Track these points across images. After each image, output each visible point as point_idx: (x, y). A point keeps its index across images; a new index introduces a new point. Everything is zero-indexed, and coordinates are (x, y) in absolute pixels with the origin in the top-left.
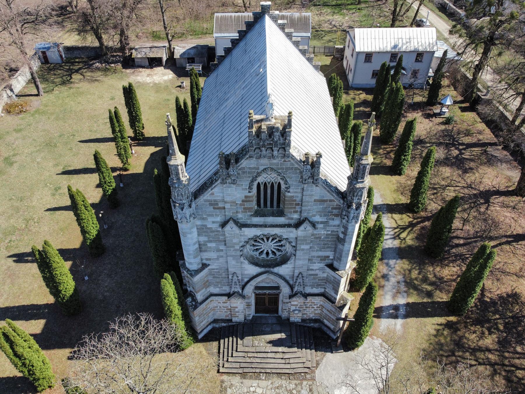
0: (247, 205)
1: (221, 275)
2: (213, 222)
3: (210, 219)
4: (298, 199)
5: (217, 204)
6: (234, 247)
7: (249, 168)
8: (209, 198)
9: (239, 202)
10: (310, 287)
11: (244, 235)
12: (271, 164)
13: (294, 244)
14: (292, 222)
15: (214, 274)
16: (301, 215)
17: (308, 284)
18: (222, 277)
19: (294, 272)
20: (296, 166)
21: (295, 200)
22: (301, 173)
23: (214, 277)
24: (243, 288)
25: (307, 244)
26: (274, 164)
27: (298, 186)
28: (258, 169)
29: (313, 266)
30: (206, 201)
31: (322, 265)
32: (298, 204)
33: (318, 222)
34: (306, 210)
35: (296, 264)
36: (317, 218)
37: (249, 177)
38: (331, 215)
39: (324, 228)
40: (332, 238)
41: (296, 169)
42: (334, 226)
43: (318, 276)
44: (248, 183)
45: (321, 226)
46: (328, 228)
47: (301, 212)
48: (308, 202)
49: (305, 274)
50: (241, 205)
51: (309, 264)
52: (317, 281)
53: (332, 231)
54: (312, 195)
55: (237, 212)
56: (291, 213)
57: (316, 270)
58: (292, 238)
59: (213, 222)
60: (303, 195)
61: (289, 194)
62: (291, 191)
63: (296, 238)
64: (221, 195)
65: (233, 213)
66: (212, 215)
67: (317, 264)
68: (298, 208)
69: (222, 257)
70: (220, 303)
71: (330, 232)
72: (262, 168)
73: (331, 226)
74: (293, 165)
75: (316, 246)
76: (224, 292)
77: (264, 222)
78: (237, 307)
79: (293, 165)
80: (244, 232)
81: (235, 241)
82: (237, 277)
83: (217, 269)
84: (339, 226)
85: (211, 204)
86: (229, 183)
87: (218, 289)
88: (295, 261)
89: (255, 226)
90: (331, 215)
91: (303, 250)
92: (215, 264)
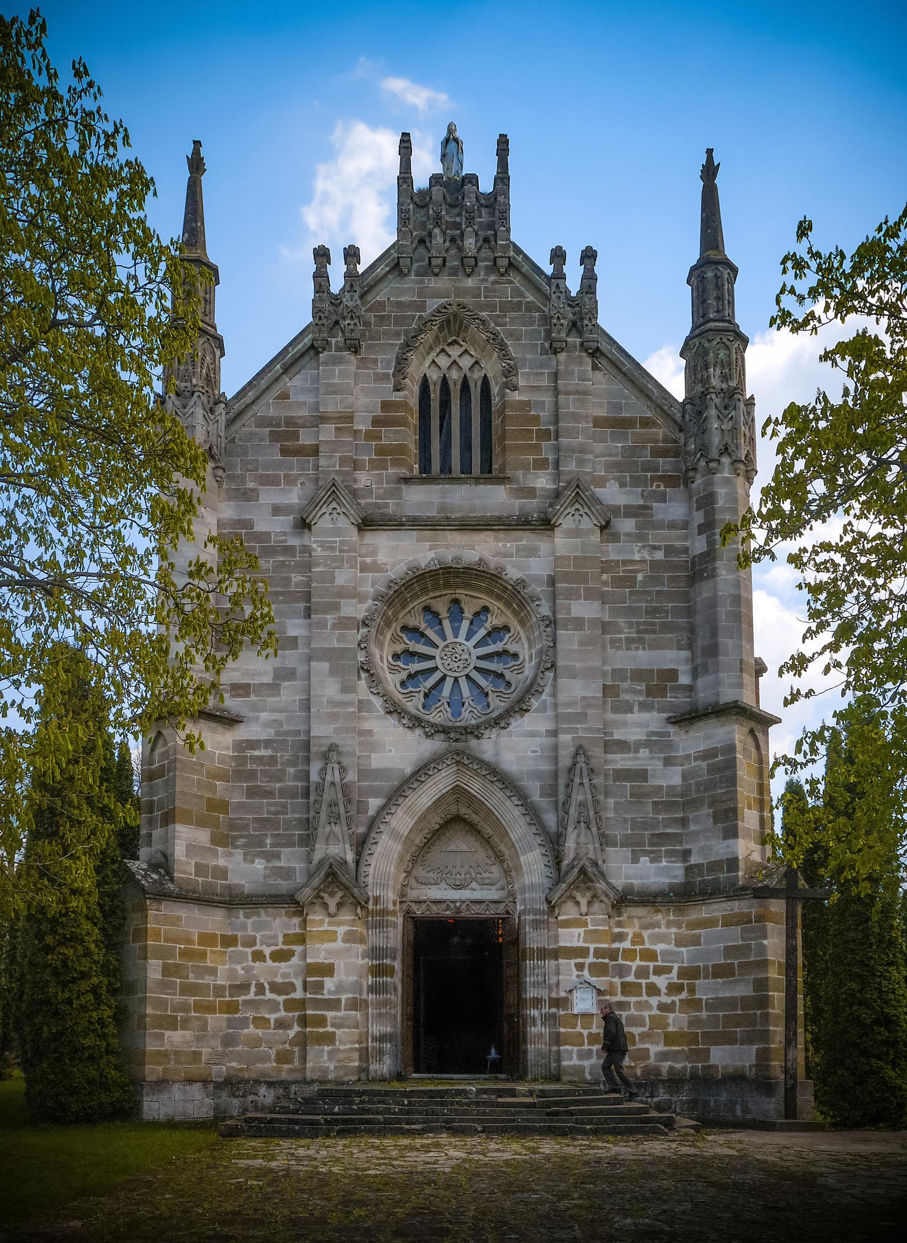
0: (389, 437)
1: (279, 777)
2: (277, 510)
3: (269, 497)
4: (545, 414)
5: (295, 436)
6: (336, 607)
7: (399, 304)
8: (272, 412)
9: (362, 426)
10: (627, 852)
11: (375, 567)
12: (459, 292)
13: (545, 610)
14: (533, 505)
15: (252, 775)
16: (557, 476)
17: (617, 833)
18: (283, 792)
19: (556, 760)
20: (531, 298)
21: (536, 420)
22: (546, 320)
23: (252, 792)
24: (361, 844)
25: (590, 595)
26: (466, 292)
27: (541, 366)
28: (422, 307)
29: (624, 724)
30: (263, 422)
31: (654, 720)
32: (545, 435)
33: (615, 510)
34: (572, 450)
35: (562, 697)
36: (613, 494)
37: (397, 335)
38: (653, 479)
39: (640, 537)
40: (672, 579)
41: (530, 307)
42: (672, 525)
43: (652, 782)
44: (392, 357)
45: (627, 525)
46: (654, 536)
47: (557, 463)
48: (576, 417)
49: (596, 752)
50: (370, 436)
51: (610, 716)
52: (647, 811)
53: (669, 550)
54: (586, 393)
55: (356, 466)
56: (525, 467)
57: (638, 745)
58: (537, 579)
59: (277, 510)
60: (556, 391)
61: (516, 396)
62: (522, 382)
63: (552, 581)
64: (310, 399)
65: (343, 461)
66: (273, 481)
67: (637, 716)
68: (547, 451)
69: (290, 674)
70: (258, 956)
71: (660, 555)
72: (433, 304)
73: (660, 525)
74: (517, 293)
75: (621, 621)
76: (283, 886)
77: (443, 508)
78: (328, 970)
79: (520, 294)
80: (374, 553)
81: (342, 578)
82: (343, 770)
83: (268, 743)
84: (685, 525)
85: (275, 437)
86: (338, 349)
87: (260, 865)
88: (554, 695)
89: (416, 523)
90: (653, 479)
91: (579, 623)
92: (264, 716)
